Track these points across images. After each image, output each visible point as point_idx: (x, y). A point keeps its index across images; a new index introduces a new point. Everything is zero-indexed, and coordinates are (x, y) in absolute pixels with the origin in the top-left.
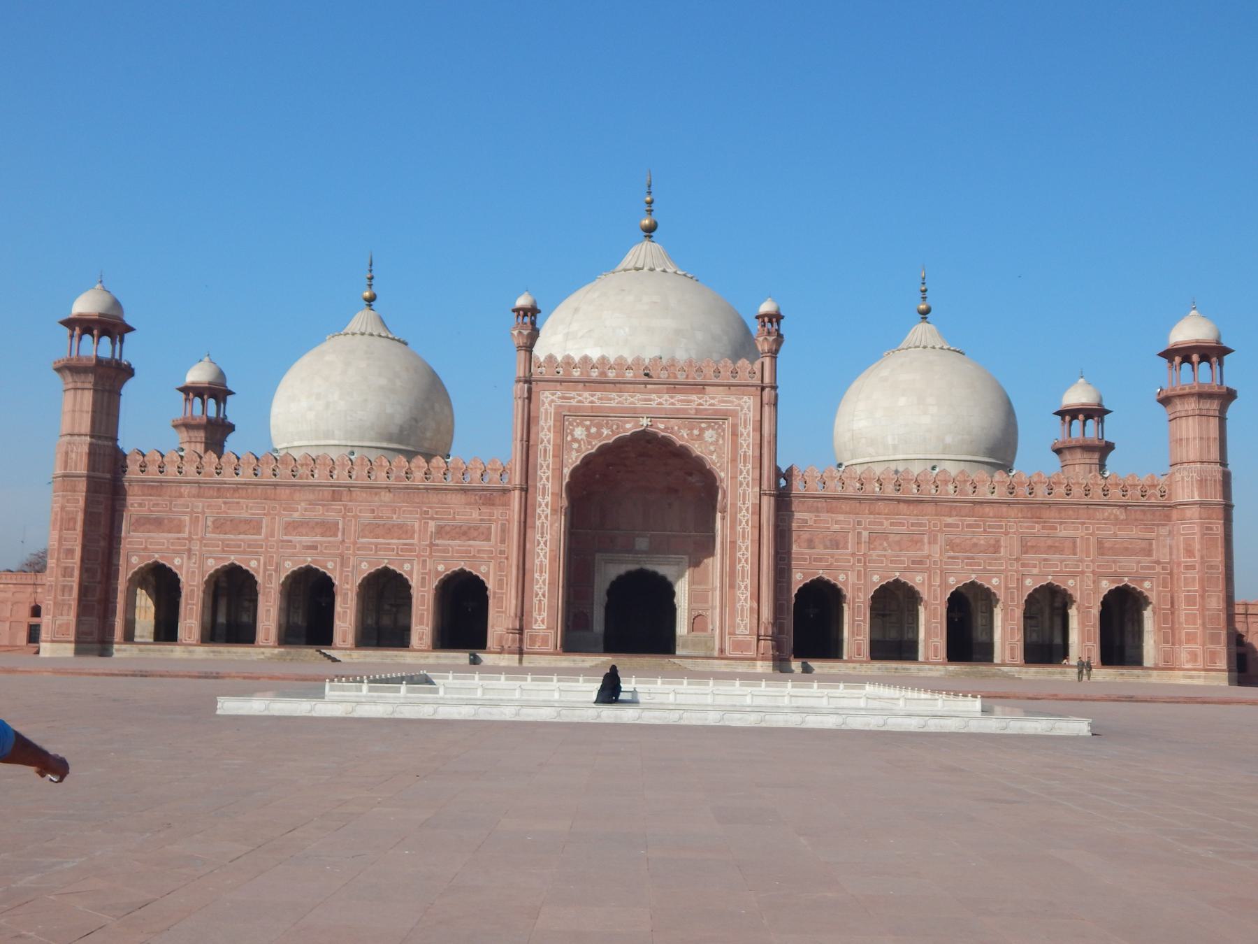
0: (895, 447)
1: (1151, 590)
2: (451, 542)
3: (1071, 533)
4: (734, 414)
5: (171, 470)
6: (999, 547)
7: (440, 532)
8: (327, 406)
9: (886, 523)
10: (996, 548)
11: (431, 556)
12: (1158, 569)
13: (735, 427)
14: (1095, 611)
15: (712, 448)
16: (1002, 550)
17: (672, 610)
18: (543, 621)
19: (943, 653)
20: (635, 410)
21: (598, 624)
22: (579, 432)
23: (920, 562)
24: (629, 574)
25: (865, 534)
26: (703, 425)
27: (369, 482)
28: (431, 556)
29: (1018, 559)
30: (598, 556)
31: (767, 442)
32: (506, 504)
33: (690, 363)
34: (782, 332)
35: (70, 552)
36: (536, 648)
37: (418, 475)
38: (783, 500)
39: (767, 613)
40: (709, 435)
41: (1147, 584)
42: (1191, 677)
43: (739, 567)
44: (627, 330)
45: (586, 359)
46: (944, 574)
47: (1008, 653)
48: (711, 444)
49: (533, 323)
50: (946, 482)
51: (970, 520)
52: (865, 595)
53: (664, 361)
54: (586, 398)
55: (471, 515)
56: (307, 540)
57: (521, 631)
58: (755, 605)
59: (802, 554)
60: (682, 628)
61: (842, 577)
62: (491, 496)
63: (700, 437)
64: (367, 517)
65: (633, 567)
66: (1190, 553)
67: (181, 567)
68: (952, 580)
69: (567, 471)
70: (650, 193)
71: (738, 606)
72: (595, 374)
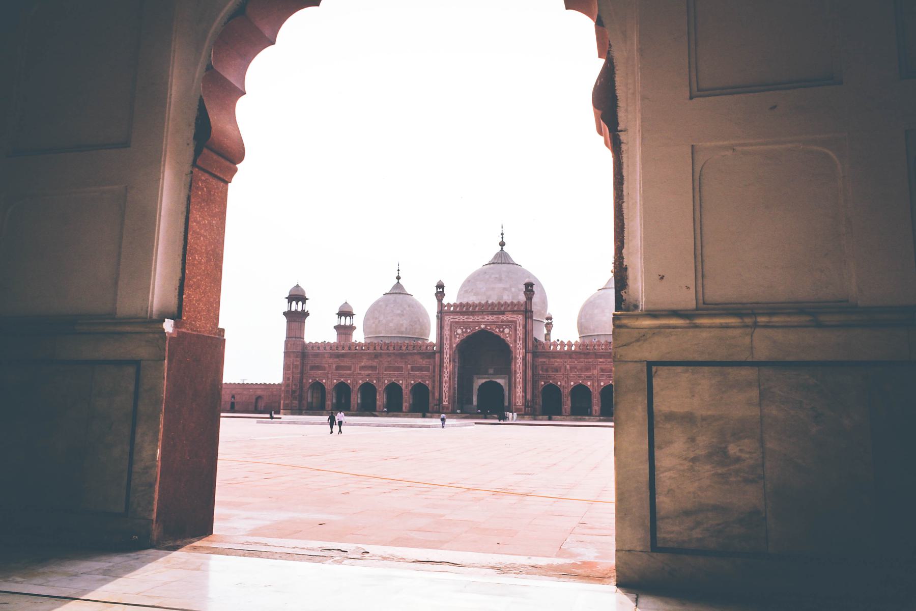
4: (515, 322)
17: (503, 395)
21: (475, 403)
22: (459, 331)
25: (568, 367)
31: (527, 332)
32: (434, 358)
33: (499, 303)
35: (289, 379)
37: (404, 348)
38: (535, 355)
39: (529, 397)
40: (507, 331)
46: (599, 381)
50: (599, 345)
56: (366, 372)
60: (506, 404)
62: (431, 355)
64: (386, 364)
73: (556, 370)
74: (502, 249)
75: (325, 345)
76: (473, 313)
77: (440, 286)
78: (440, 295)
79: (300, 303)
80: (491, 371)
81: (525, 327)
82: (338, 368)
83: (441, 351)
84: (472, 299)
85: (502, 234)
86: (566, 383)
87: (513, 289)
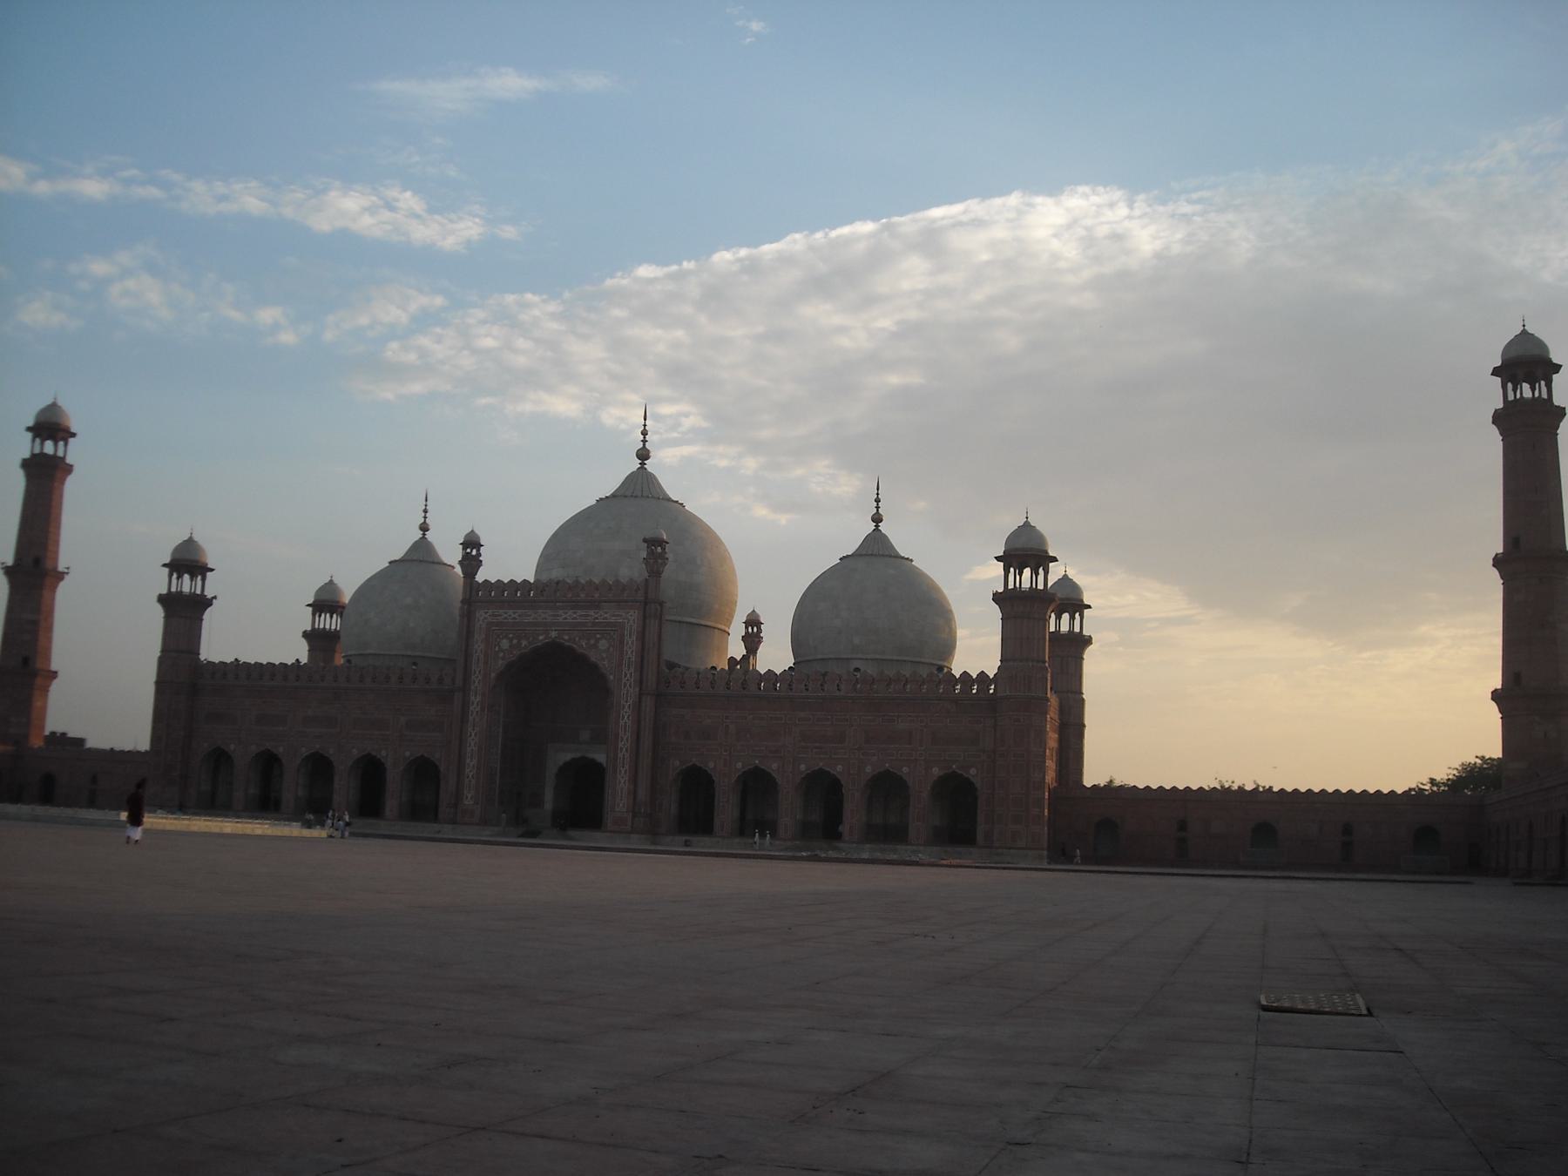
13: (622, 636)
21: (549, 805)
22: (505, 644)
33: (590, 582)
49: (479, 554)
61: (711, 765)
65: (578, 755)
74: (643, 464)
75: (239, 670)
77: (472, 543)
78: (471, 562)
81: (642, 636)
84: (556, 574)
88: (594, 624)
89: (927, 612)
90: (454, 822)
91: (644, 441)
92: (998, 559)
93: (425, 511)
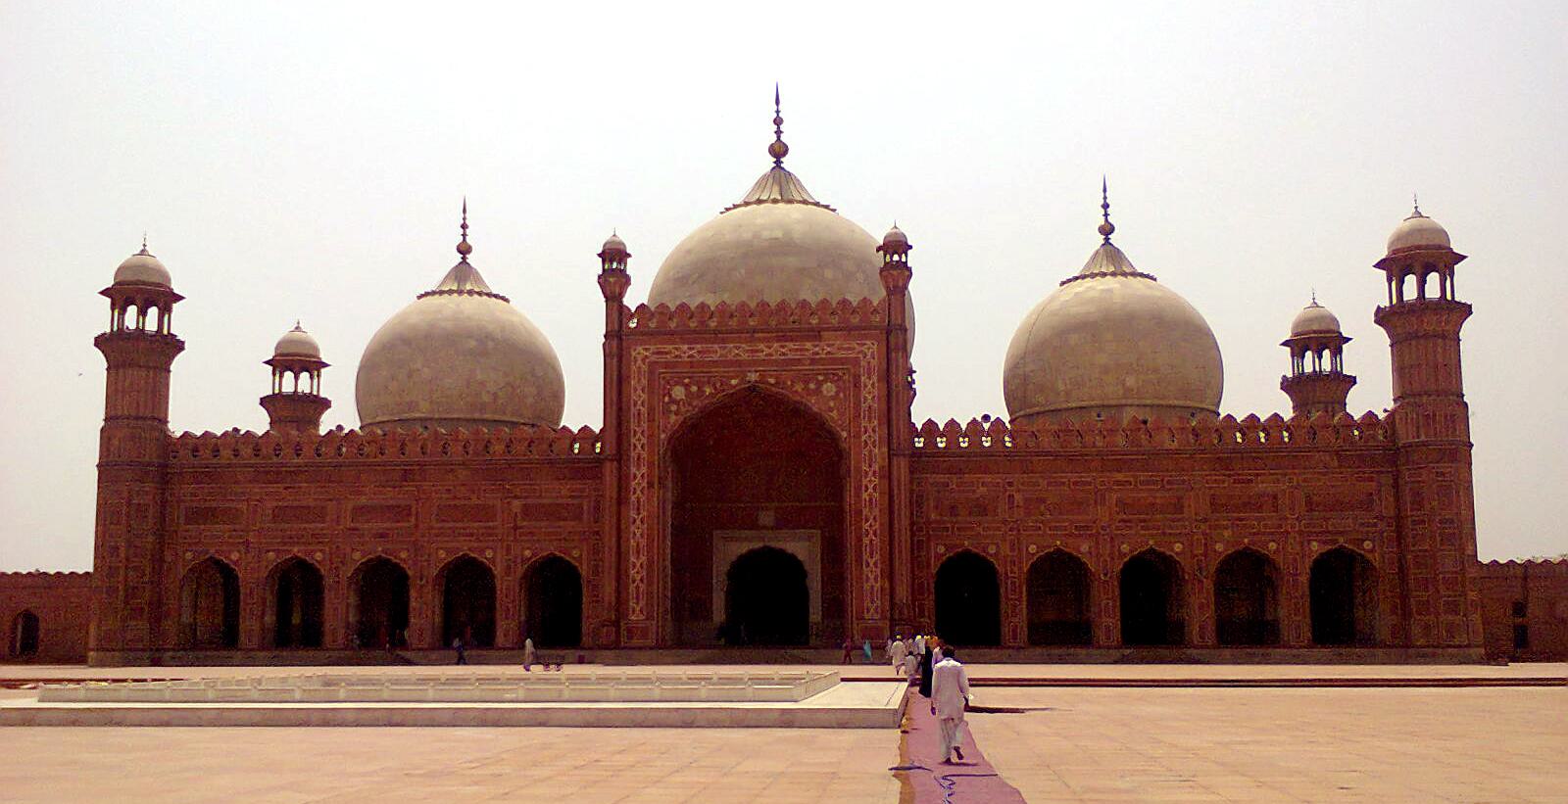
0: (1068, 394)
1: (1372, 551)
2: (538, 524)
3: (1270, 488)
4: (856, 362)
5: (226, 453)
6: (1182, 507)
7: (527, 511)
8: (410, 376)
9: (1043, 483)
10: (1178, 508)
11: (515, 540)
12: (1382, 526)
14: (1304, 579)
15: (832, 404)
16: (1186, 510)
17: (804, 594)
18: (641, 611)
19: (1116, 635)
20: (739, 363)
21: (719, 615)
22: (679, 392)
23: (1087, 527)
24: (752, 552)
25: (1018, 497)
26: (821, 378)
27: (445, 458)
28: (515, 540)
29: (1205, 520)
30: (717, 533)
33: (804, 304)
34: (909, 265)
36: (635, 642)
37: (498, 448)
39: (903, 593)
40: (829, 389)
41: (1368, 545)
42: (1424, 656)
43: (866, 541)
44: (743, 271)
45: (683, 307)
47: (1196, 629)
48: (833, 398)
49: (623, 272)
51: (1143, 476)
52: (1020, 569)
53: (773, 305)
54: (685, 351)
55: (556, 491)
57: (617, 624)
58: (887, 585)
59: (944, 522)
60: (815, 615)
61: (992, 550)
63: (818, 391)
65: (757, 545)
66: (1419, 504)
67: (236, 563)
68: (1125, 548)
69: (663, 436)
70: (778, 112)
71: (867, 586)
72: (693, 325)
73: (982, 509)
74: (778, 163)
75: (236, 440)
76: (719, 336)
77: (614, 256)
79: (153, 312)
80: (766, 518)
81: (887, 376)
82: (279, 515)
83: (620, 456)
85: (778, 121)
86: (1012, 550)
87: (829, 274)
88: (813, 361)
89: (1189, 344)
90: (615, 645)
91: (779, 133)
92: (1378, 265)
93: (464, 226)
